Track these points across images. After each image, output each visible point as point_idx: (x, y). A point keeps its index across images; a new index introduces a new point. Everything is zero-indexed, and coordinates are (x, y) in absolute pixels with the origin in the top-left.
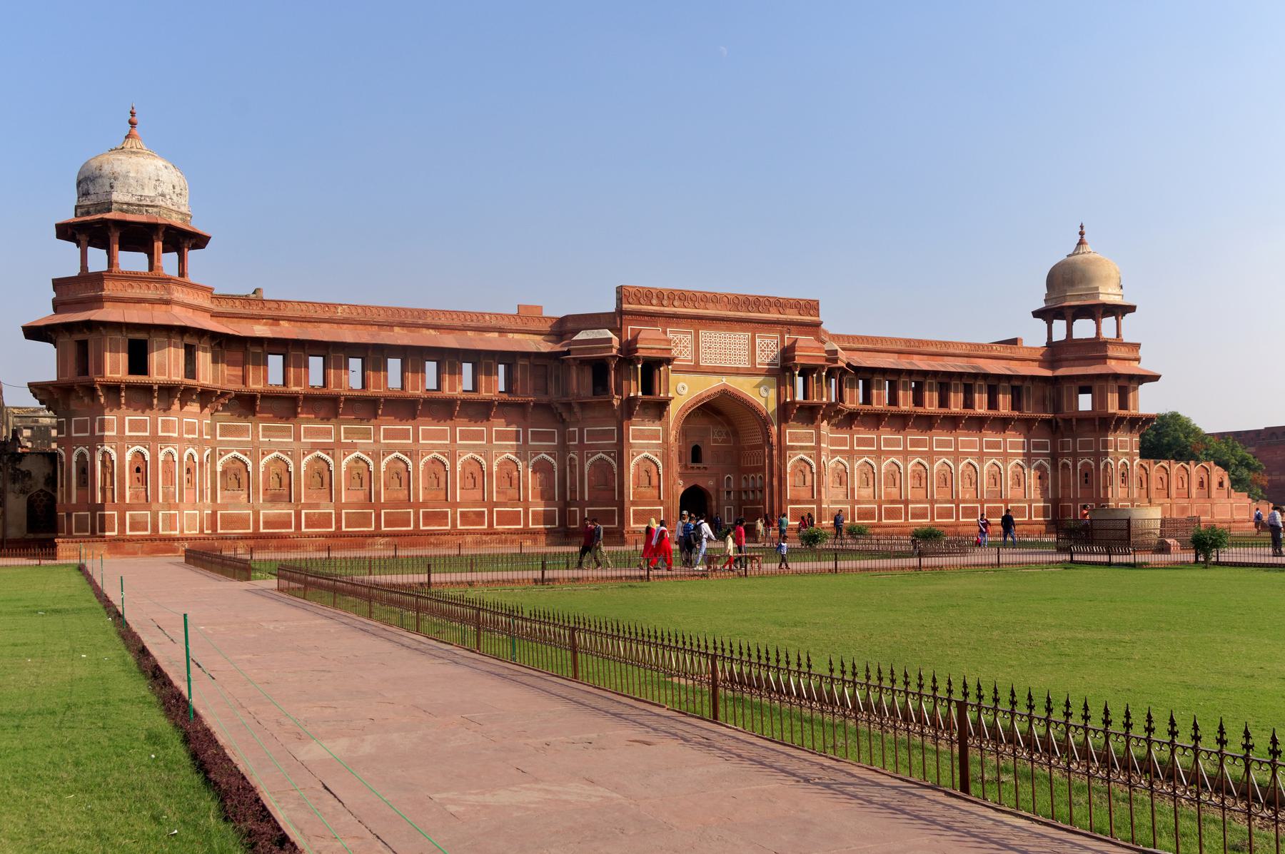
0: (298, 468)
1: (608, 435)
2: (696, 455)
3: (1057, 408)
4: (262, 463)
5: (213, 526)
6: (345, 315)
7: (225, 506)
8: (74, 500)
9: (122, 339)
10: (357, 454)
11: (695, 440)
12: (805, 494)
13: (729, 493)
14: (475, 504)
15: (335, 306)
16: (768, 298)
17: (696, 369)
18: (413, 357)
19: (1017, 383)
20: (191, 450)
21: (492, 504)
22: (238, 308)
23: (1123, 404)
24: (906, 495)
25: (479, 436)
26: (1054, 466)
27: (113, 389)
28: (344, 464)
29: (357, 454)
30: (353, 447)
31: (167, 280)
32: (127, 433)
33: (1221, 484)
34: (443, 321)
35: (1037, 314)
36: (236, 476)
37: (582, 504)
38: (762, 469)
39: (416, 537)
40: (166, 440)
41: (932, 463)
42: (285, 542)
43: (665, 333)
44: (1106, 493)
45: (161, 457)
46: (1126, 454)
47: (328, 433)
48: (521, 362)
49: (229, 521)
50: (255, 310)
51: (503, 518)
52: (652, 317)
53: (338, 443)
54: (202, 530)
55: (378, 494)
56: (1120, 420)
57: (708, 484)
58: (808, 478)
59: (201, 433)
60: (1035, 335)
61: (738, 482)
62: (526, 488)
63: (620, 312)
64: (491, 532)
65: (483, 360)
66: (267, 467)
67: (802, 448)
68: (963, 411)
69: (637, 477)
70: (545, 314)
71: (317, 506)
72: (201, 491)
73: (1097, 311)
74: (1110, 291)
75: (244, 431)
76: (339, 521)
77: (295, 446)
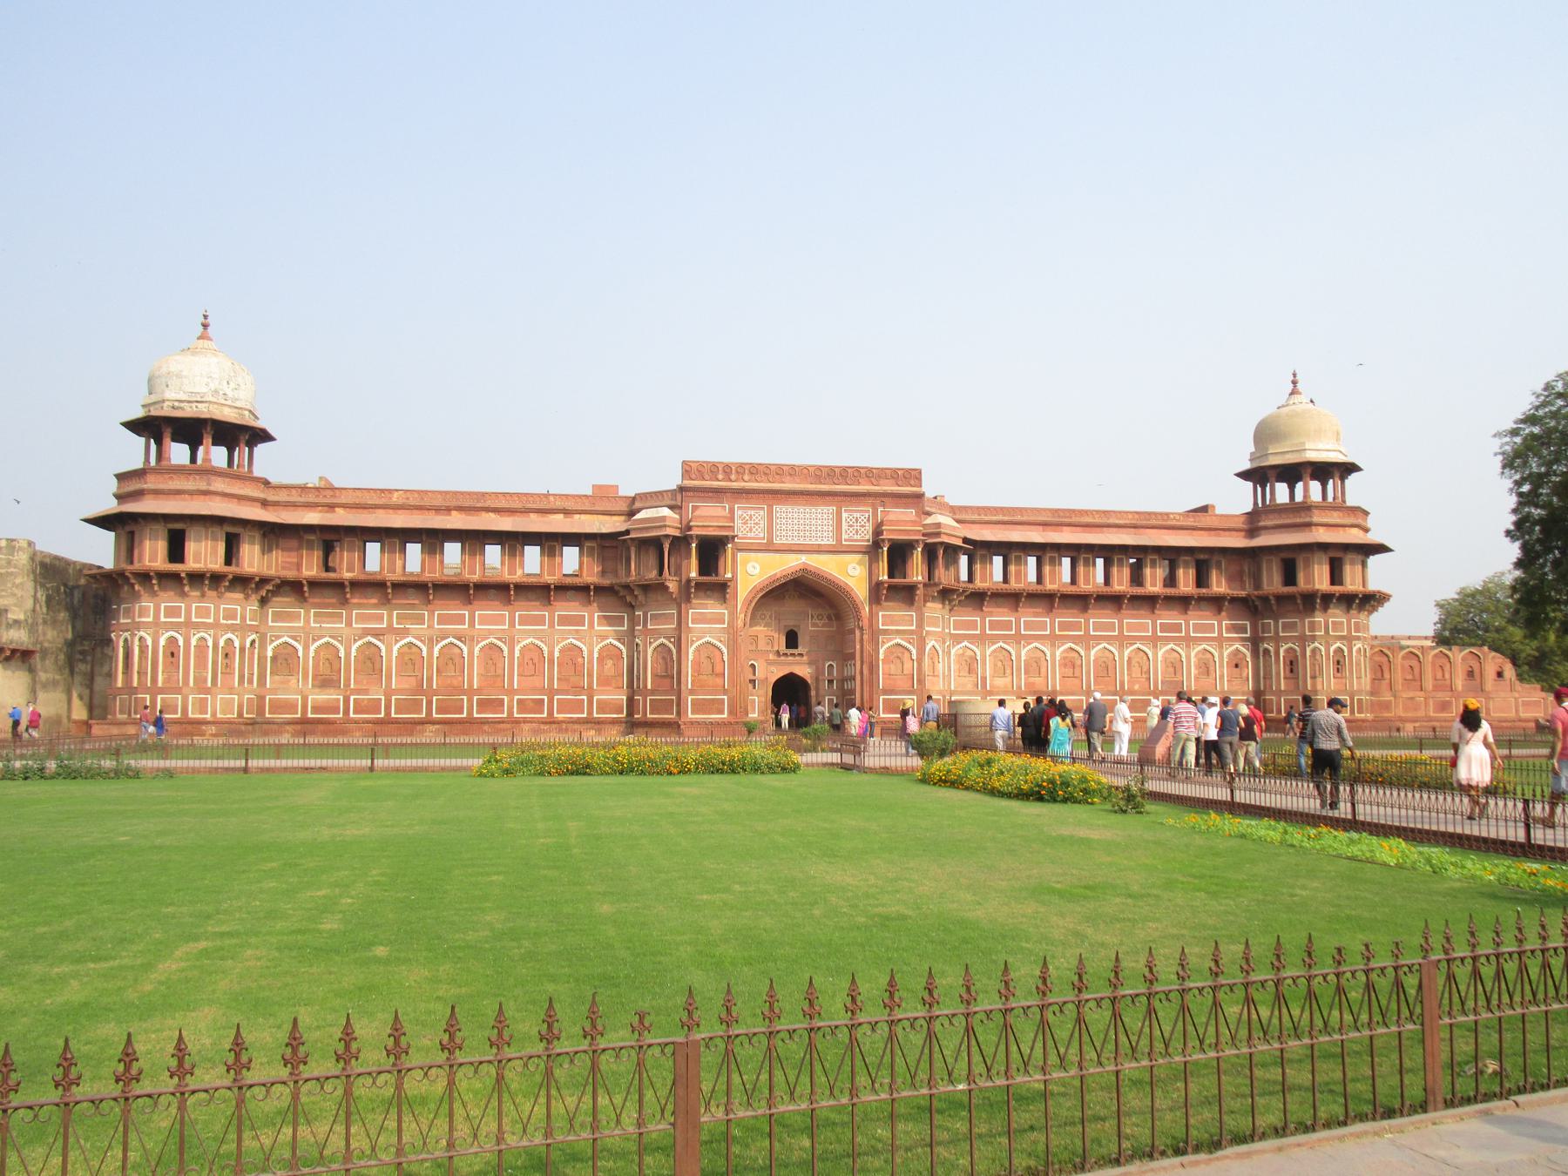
0: (348, 654)
1: (667, 618)
2: (792, 640)
3: (1258, 586)
4: (313, 648)
5: (261, 711)
6: (400, 502)
7: (274, 691)
8: (120, 684)
9: (162, 531)
10: (410, 639)
11: (791, 623)
12: (902, 683)
13: (830, 682)
14: (534, 690)
15: (390, 491)
16: (857, 469)
17: (769, 548)
18: (474, 540)
19: (1202, 557)
20: (230, 635)
21: (551, 693)
22: (295, 497)
23: (1336, 578)
24: (1054, 685)
25: (540, 621)
26: (1255, 653)
27: (145, 577)
28: (395, 649)
29: (410, 639)
30: (406, 632)
31: (179, 470)
32: (163, 619)
33: (1500, 674)
34: (503, 504)
35: (1244, 475)
36: (285, 660)
37: (645, 692)
38: (853, 656)
39: (470, 724)
40: (198, 626)
41: (1088, 649)
42: (331, 727)
43: (732, 511)
44: (1314, 685)
45: (194, 642)
46: (1341, 638)
47: (380, 618)
48: (588, 544)
49: (277, 706)
50: (311, 498)
51: (564, 707)
52: (717, 493)
53: (390, 629)
54: (240, 714)
55: (430, 679)
56: (1327, 599)
57: (804, 671)
58: (908, 665)
59: (243, 618)
60: (1239, 499)
61: (841, 671)
62: (590, 675)
63: (682, 489)
64: (551, 721)
65: (551, 542)
66: (317, 651)
67: (898, 632)
68: (325, 575)
69: (697, 664)
70: (621, 493)
71: (366, 692)
72: (242, 677)
73: (1323, 471)
74: (1321, 446)
75: (297, 617)
76: (388, 707)
77: (347, 631)
